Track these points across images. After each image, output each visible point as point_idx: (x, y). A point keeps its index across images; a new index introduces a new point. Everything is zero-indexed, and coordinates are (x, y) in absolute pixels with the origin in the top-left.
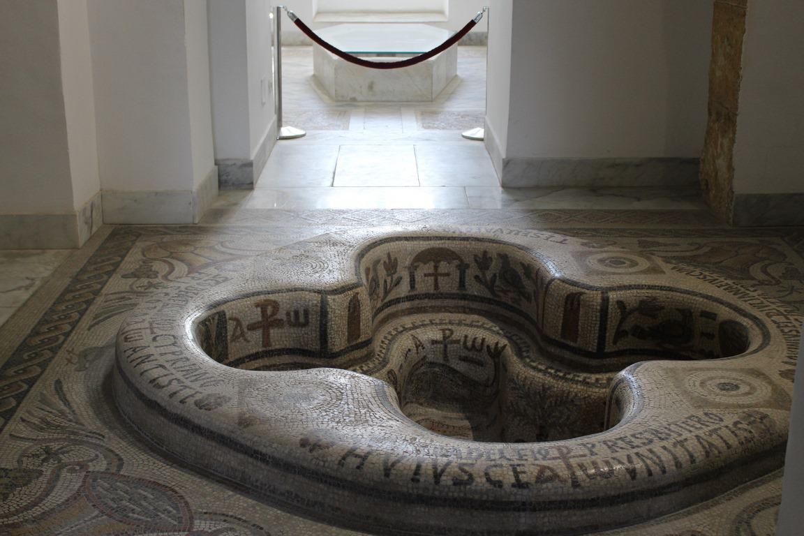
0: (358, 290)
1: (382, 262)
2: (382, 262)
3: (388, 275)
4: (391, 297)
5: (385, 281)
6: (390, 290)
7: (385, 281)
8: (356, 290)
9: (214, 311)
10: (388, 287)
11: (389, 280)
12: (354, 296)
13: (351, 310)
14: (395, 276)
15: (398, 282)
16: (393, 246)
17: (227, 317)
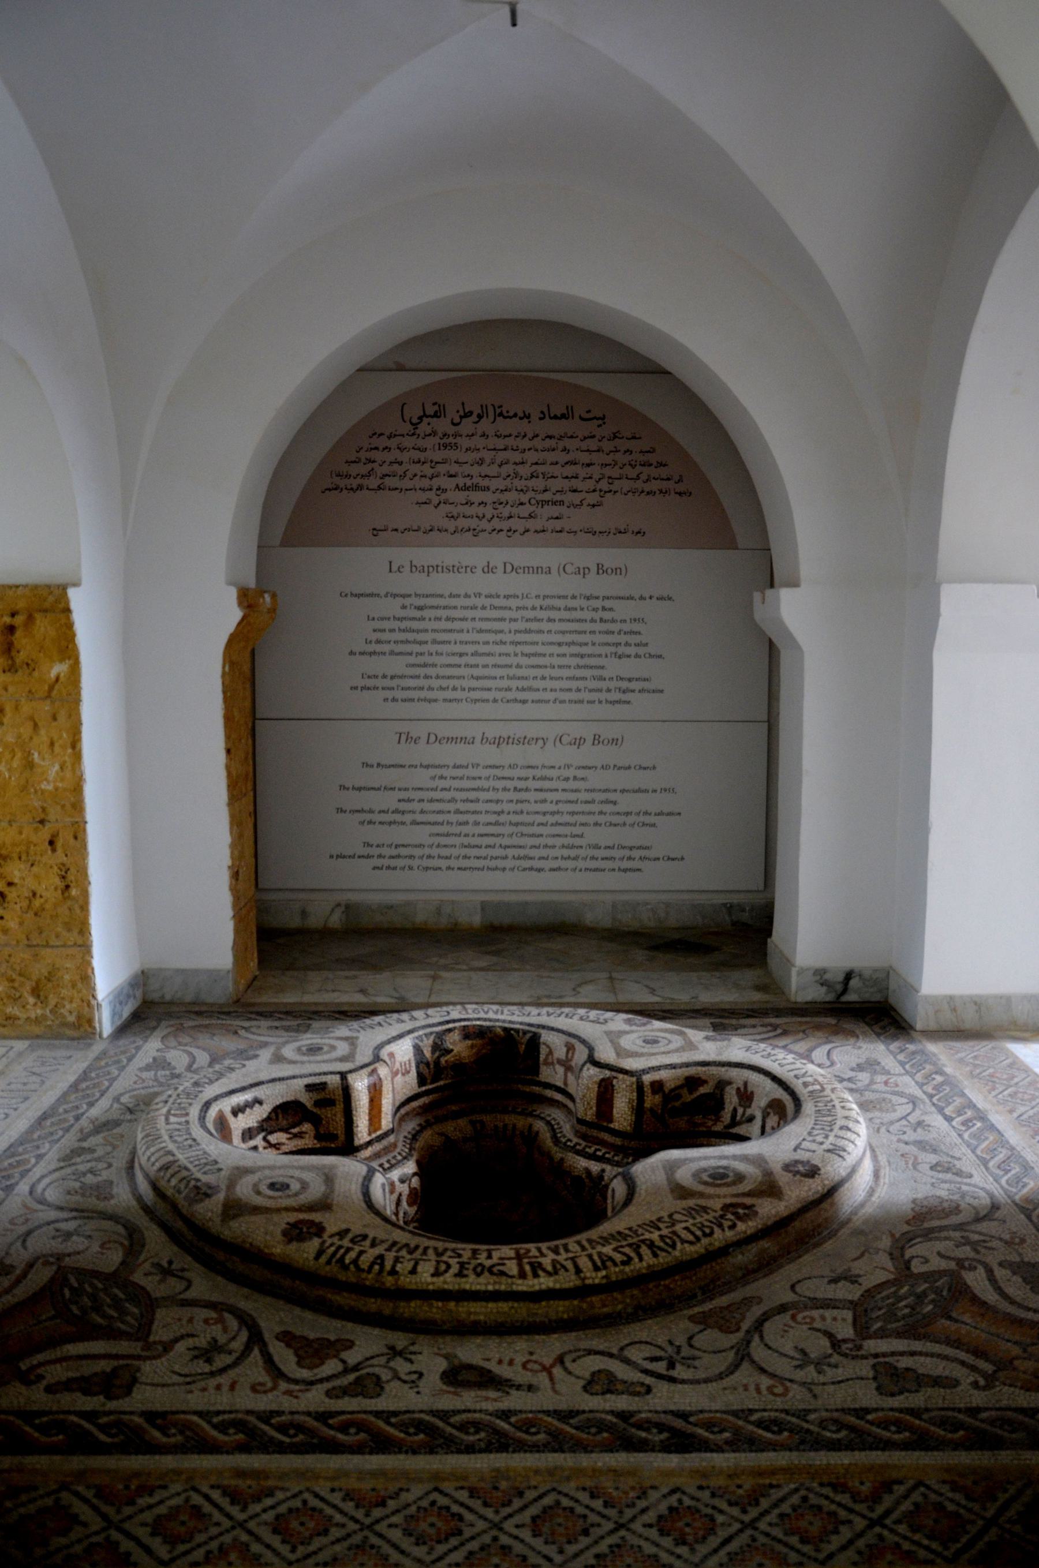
0: (621, 1076)
1: (735, 1086)
2: (735, 1086)
3: (740, 1105)
4: (735, 1130)
5: (735, 1110)
6: (740, 1123)
7: (735, 1110)
8: (614, 1074)
9: (533, 1029)
10: (738, 1118)
11: (740, 1111)
12: (609, 1078)
13: (602, 1089)
14: (749, 1112)
15: (751, 1119)
16: (754, 1077)
17: (542, 1040)
